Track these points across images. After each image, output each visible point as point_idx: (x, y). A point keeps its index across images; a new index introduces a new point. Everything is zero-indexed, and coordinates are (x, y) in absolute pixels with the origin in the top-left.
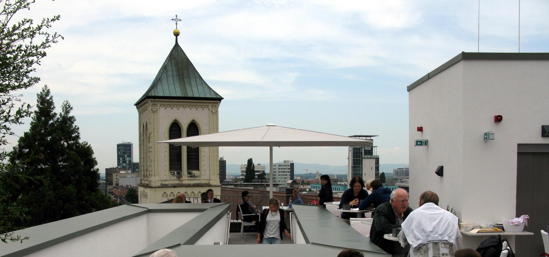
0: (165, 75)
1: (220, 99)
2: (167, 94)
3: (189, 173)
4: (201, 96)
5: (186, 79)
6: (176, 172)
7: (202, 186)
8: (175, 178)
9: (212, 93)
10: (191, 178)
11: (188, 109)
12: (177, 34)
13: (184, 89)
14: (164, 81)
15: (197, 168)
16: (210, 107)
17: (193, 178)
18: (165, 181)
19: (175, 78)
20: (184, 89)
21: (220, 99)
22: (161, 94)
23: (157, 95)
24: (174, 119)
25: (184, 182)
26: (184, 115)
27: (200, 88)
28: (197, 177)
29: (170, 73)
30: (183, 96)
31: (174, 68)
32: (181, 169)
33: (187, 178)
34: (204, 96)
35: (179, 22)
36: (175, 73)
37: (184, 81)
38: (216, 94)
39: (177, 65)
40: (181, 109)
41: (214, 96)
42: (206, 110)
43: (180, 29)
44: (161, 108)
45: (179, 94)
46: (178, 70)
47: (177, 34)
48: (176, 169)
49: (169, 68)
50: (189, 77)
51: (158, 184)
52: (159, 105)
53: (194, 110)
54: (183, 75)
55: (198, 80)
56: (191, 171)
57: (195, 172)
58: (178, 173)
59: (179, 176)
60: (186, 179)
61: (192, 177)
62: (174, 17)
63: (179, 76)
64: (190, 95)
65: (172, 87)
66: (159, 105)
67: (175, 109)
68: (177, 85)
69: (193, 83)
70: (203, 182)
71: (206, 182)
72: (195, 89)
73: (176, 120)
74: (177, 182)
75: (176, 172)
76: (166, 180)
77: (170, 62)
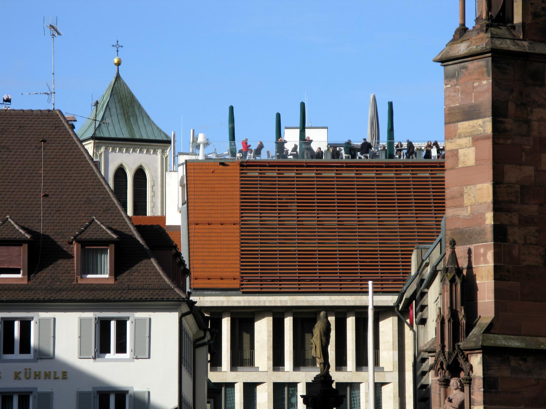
0: (108, 112)
2: (113, 136)
5: (131, 118)
9: (162, 135)
13: (131, 130)
19: (120, 116)
20: (131, 130)
22: (106, 135)
23: (102, 136)
29: (113, 110)
31: (117, 105)
34: (154, 138)
36: (119, 111)
39: (120, 101)
41: (166, 139)
45: (126, 136)
49: (112, 106)
50: (135, 116)
62: (115, 43)
64: (138, 137)
65: (117, 127)
73: (121, 165)
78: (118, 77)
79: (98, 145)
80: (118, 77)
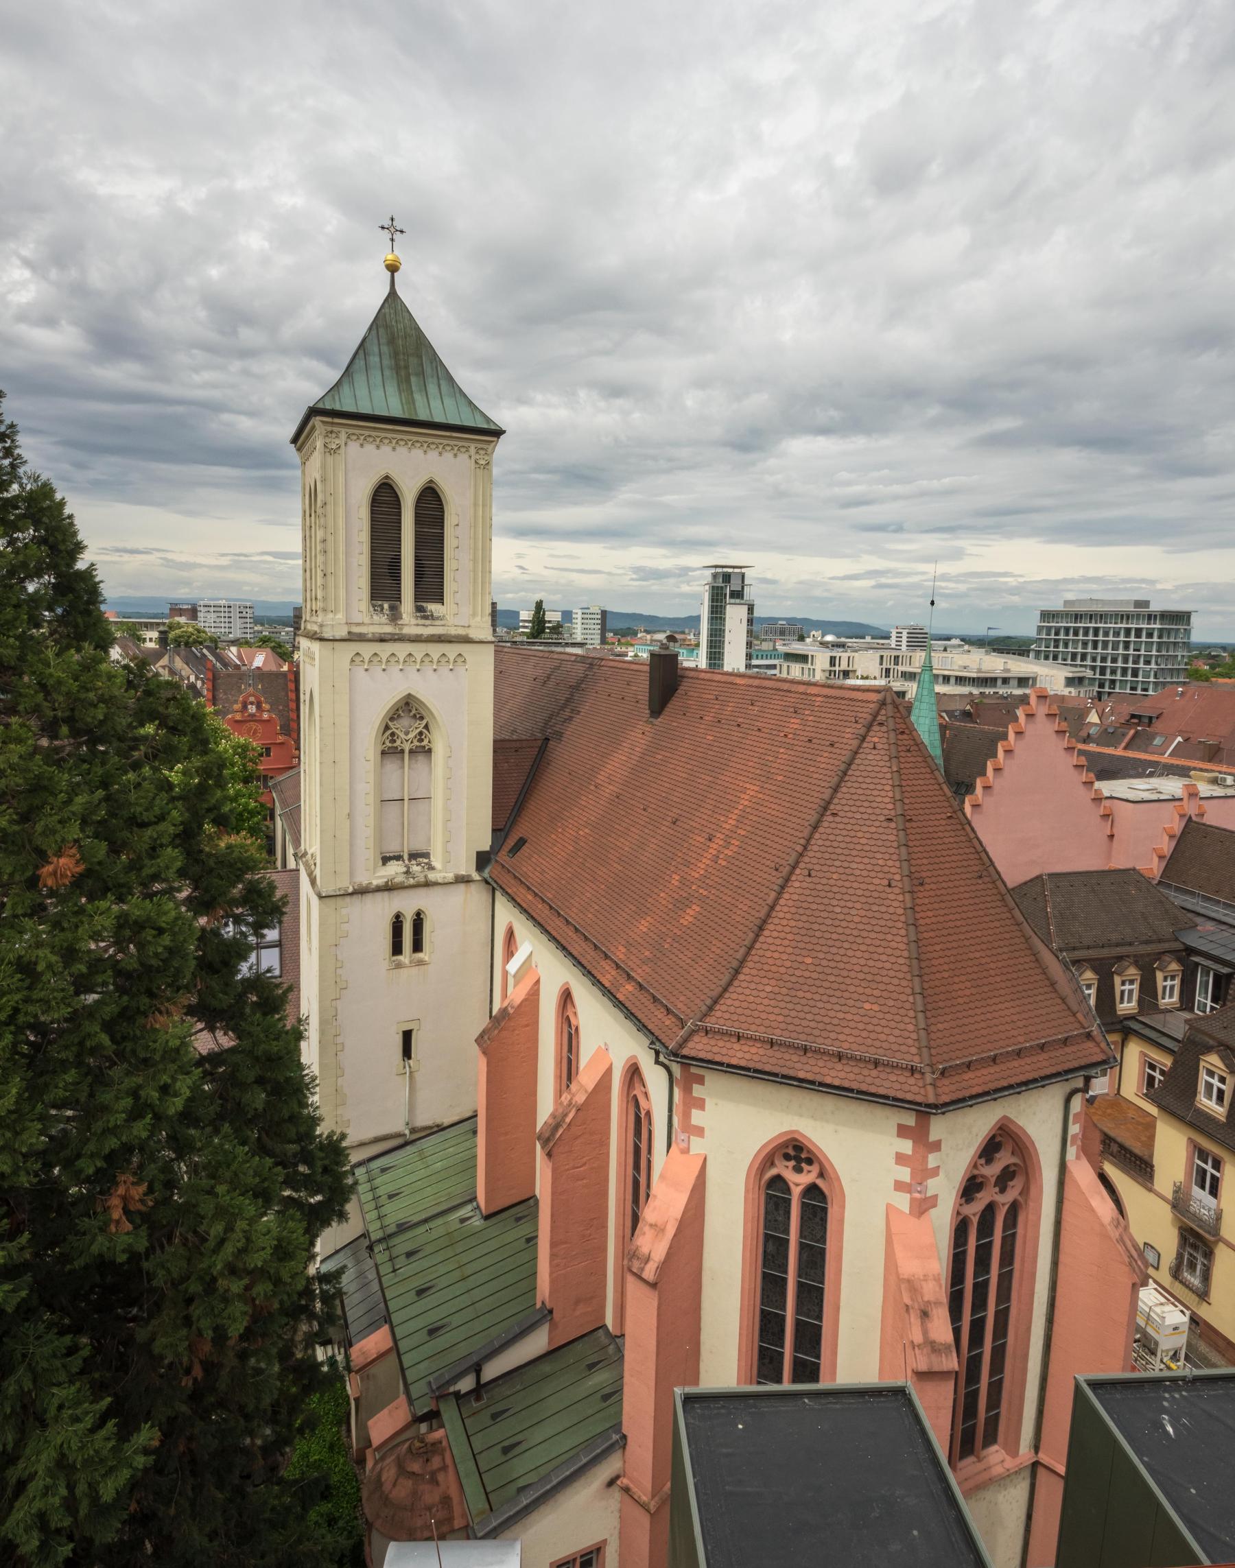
0: (360, 363)
1: (498, 433)
2: (365, 409)
3: (419, 609)
4: (452, 421)
5: (413, 379)
6: (386, 606)
7: (450, 642)
8: (384, 619)
9: (478, 417)
10: (423, 622)
11: (417, 453)
12: (393, 268)
14: (360, 379)
15: (440, 599)
16: (472, 450)
17: (428, 622)
18: (358, 624)
19: (387, 373)
21: (498, 433)
22: (349, 407)
23: (338, 407)
24: (383, 473)
25: (406, 631)
26: (411, 467)
27: (448, 402)
28: (438, 618)
29: (374, 360)
30: (406, 416)
31: (385, 349)
32: (399, 599)
33: (414, 621)
34: (458, 423)
35: (397, 236)
36: (386, 362)
37: (408, 381)
38: (488, 420)
39: (392, 341)
40: (402, 450)
42: (463, 457)
43: (400, 254)
44: (350, 443)
45: (396, 410)
46: (395, 355)
47: (393, 268)
48: (386, 599)
50: (421, 374)
51: (342, 632)
52: (343, 436)
53: (433, 455)
54: (407, 367)
55: (443, 382)
56: (424, 605)
57: (432, 607)
58: (392, 608)
59: (395, 615)
60: (410, 622)
61: (426, 618)
62: (387, 223)
63: (397, 368)
64: (423, 415)
65: (378, 393)
66: (343, 436)
67: (386, 449)
68: (392, 389)
69: (432, 389)
70: (453, 631)
71: (461, 632)
72: (435, 404)
74: (389, 629)
75: (386, 606)
76: (362, 624)
77: (374, 332)
78: (393, 295)
79: (329, 429)
80: (393, 295)
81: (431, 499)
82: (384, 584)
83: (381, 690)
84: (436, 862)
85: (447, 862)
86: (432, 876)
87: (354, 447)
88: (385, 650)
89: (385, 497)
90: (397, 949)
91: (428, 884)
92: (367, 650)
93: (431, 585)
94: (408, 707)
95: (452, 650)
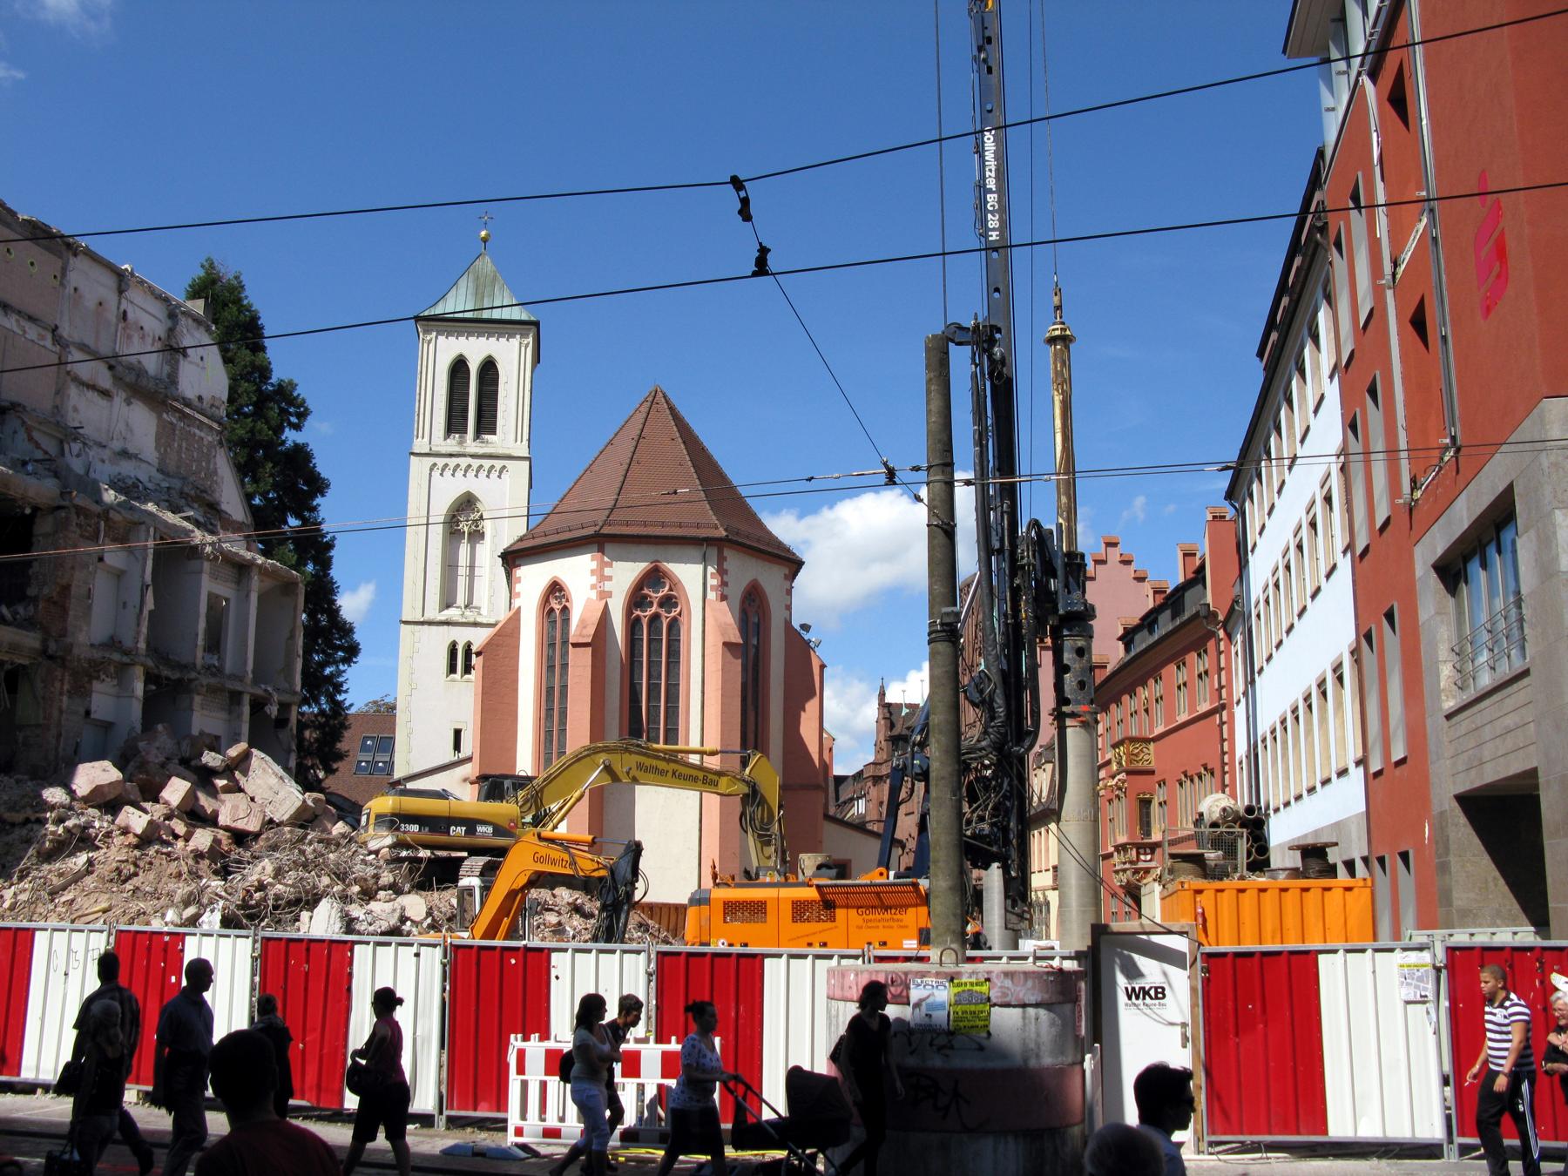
36: (471, 290)
59: (461, 443)
60: (471, 446)
74: (456, 449)
81: (489, 368)
82: (455, 424)
83: (448, 490)
84: (484, 611)
85: (491, 611)
86: (479, 620)
87: (441, 339)
88: (453, 462)
89: (459, 367)
90: (452, 669)
91: (475, 624)
92: (441, 462)
93: (487, 423)
94: (467, 503)
95: (498, 464)
